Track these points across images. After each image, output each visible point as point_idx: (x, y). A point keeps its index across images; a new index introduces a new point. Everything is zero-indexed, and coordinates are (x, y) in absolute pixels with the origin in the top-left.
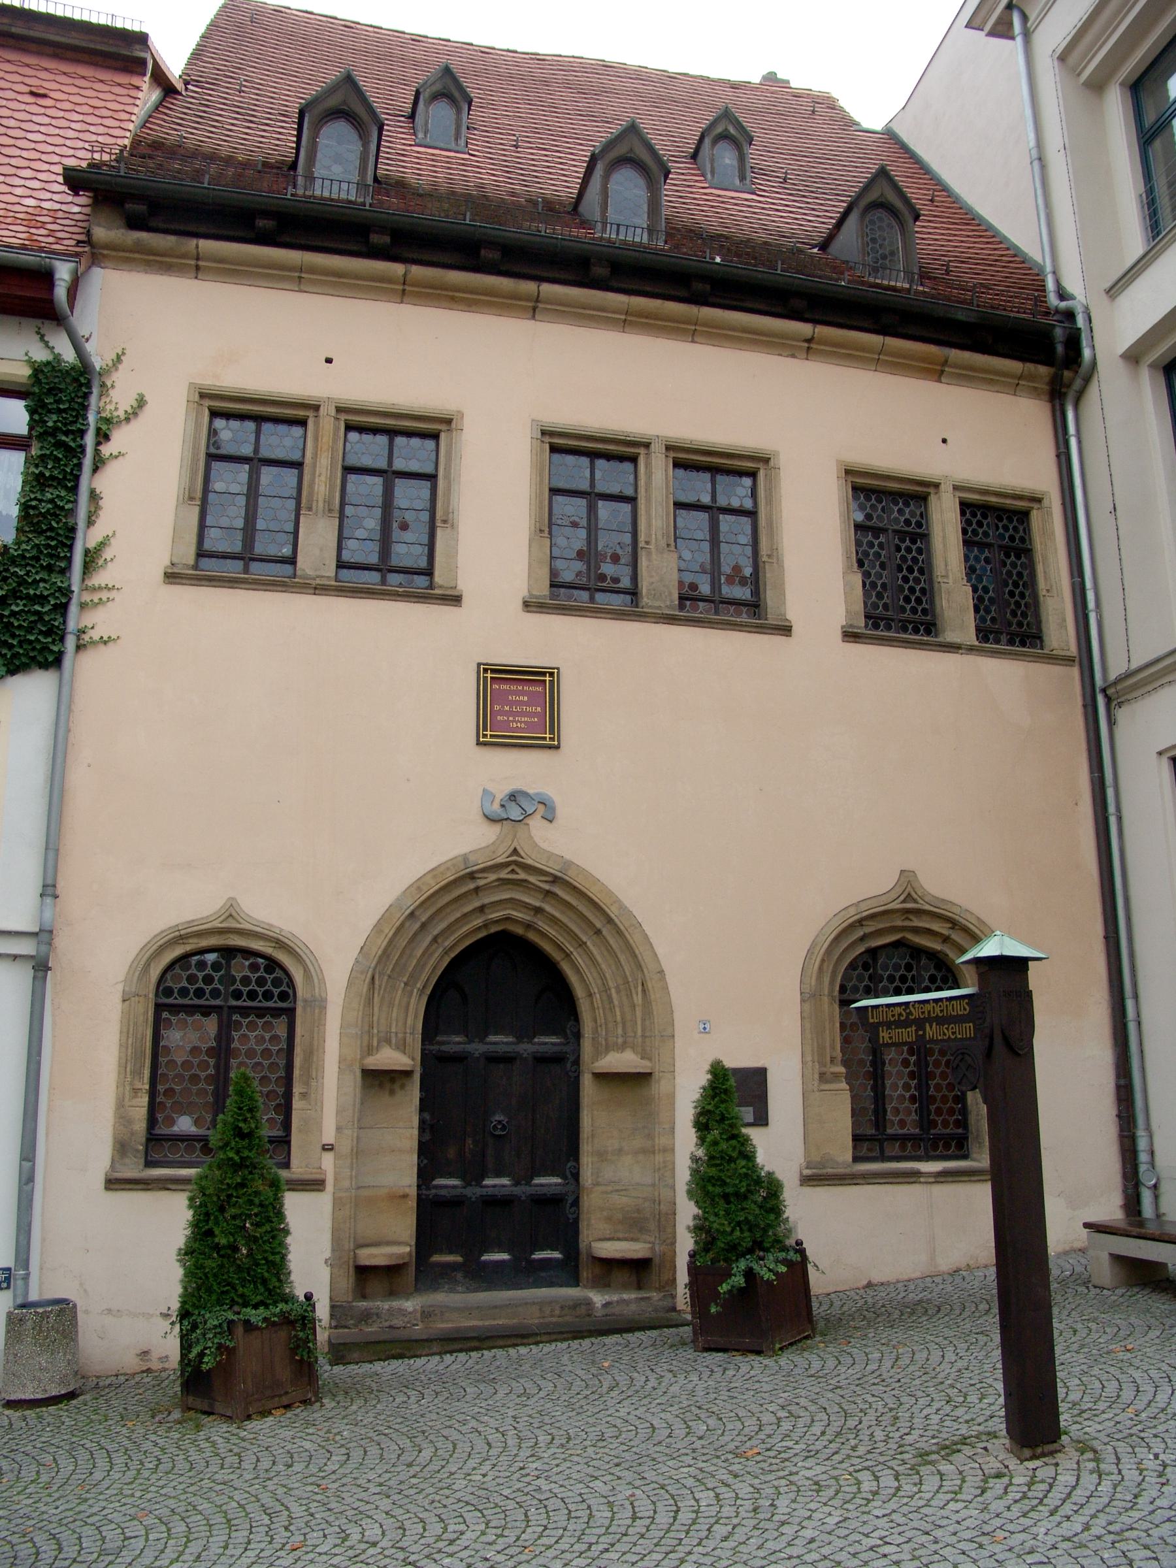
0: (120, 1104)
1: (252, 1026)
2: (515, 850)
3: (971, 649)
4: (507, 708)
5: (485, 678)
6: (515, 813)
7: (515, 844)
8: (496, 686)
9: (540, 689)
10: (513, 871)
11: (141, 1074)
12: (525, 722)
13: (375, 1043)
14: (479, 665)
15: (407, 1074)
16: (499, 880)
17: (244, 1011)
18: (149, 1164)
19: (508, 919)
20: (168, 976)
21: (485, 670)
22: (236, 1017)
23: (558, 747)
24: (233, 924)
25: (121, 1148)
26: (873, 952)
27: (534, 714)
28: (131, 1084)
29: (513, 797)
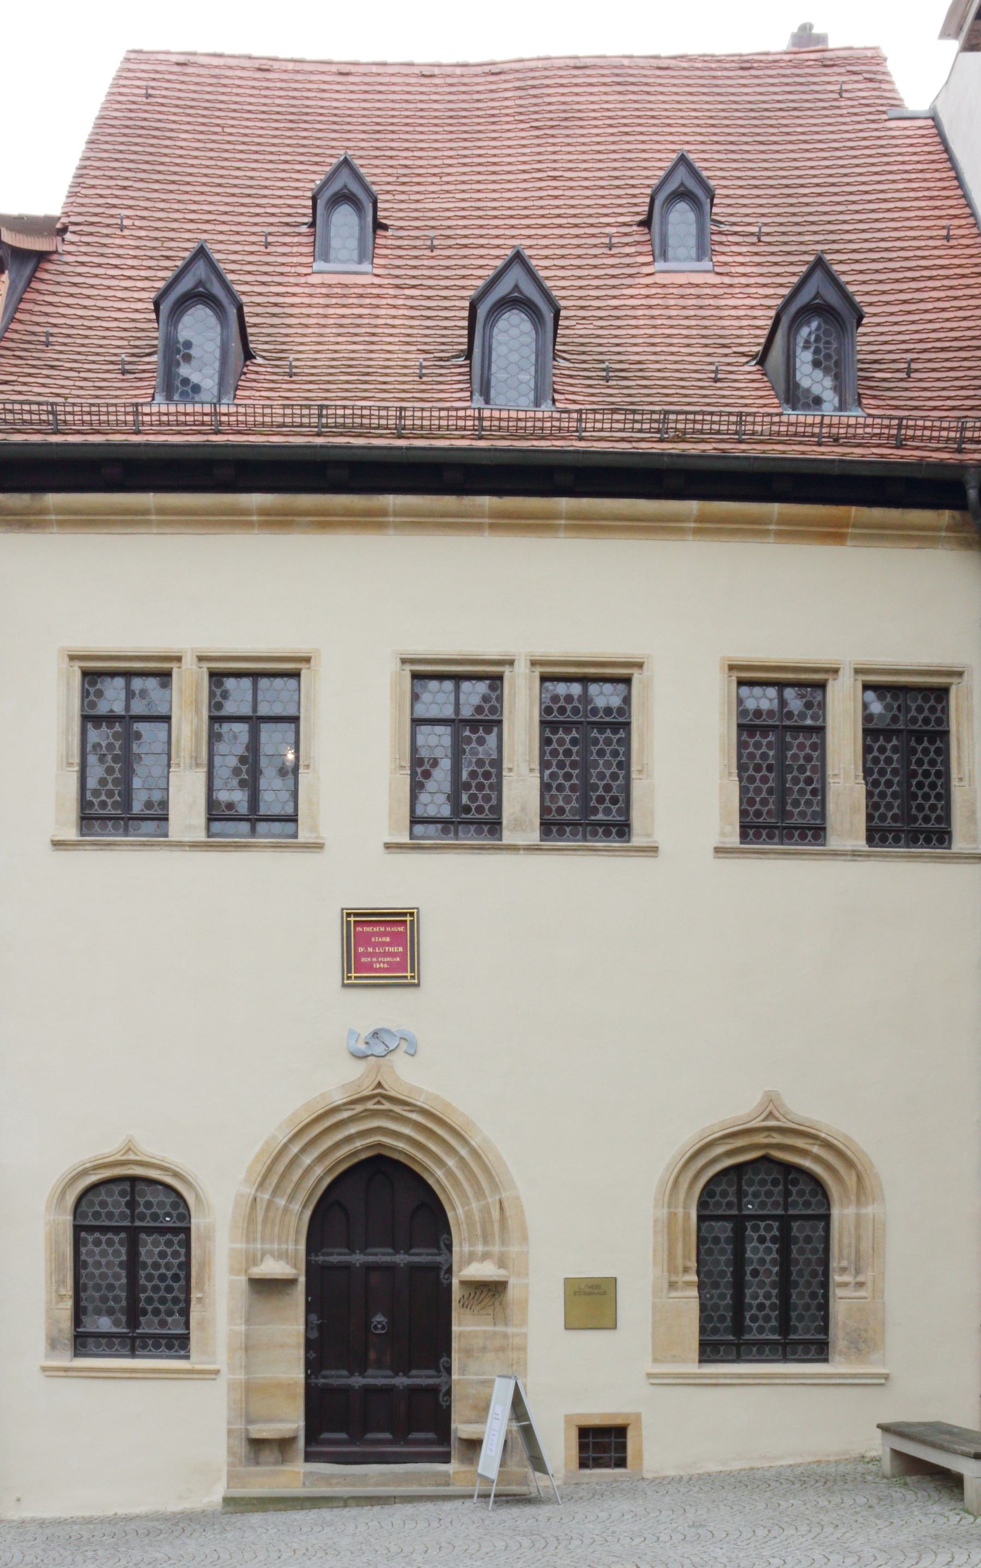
0: (49, 1310)
1: (156, 1244)
2: (379, 1085)
3: (855, 855)
4: (370, 950)
5: (348, 923)
6: (380, 1050)
7: (379, 1078)
8: (359, 929)
9: (401, 929)
10: (379, 1103)
11: (64, 1282)
12: (388, 963)
13: (259, 1256)
14: (343, 909)
15: (292, 1282)
16: (366, 1110)
17: (149, 1231)
18: (77, 1354)
19: (380, 1145)
20: (84, 1202)
21: (349, 915)
22: (143, 1236)
23: (418, 985)
24: (132, 1157)
25: (53, 1344)
26: (738, 1169)
27: (393, 955)
28: (57, 1291)
29: (375, 1034)
